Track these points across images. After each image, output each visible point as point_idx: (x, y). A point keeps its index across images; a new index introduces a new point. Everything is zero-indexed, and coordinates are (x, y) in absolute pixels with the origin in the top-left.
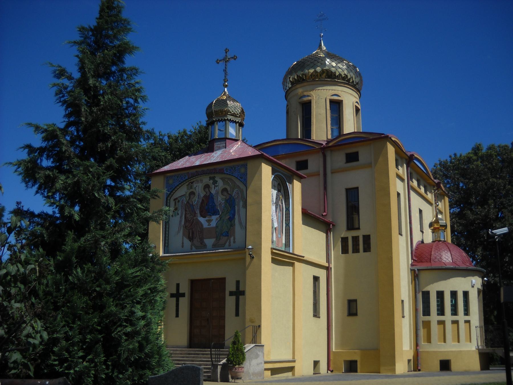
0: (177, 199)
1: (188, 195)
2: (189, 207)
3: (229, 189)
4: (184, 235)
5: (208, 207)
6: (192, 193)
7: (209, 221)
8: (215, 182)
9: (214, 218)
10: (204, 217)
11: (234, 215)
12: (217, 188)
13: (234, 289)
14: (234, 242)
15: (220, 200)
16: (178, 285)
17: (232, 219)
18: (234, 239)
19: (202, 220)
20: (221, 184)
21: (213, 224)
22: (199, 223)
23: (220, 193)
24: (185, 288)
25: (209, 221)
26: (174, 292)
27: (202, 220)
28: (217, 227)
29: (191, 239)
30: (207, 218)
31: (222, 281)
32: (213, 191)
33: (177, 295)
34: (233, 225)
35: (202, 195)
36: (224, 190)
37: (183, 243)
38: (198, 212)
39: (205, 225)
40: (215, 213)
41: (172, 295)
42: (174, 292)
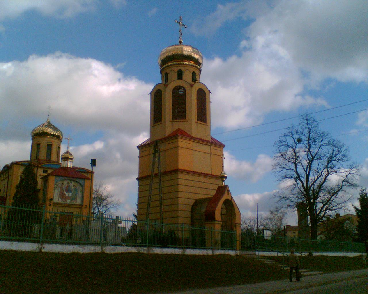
0: (57, 184)
1: (61, 184)
2: (61, 188)
3: (76, 185)
4: (59, 197)
6: (62, 184)
7: (69, 194)
9: (70, 193)
10: (67, 192)
11: (77, 194)
12: (71, 184)
14: (77, 202)
15: (73, 188)
17: (76, 195)
18: (77, 201)
19: (66, 193)
21: (70, 195)
22: (65, 194)
23: (73, 186)
25: (69, 194)
27: (66, 193)
28: (71, 196)
29: (62, 199)
30: (68, 193)
34: (77, 197)
35: (67, 185)
36: (74, 186)
37: (58, 200)
38: (64, 190)
39: (67, 195)
40: (71, 192)
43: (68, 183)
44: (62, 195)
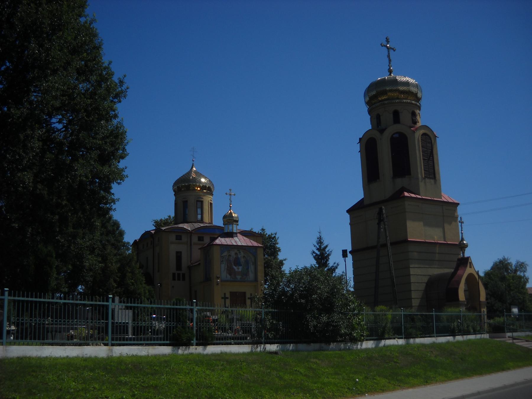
5: (237, 262)
6: (230, 255)
7: (238, 268)
8: (240, 252)
9: (240, 268)
13: (249, 297)
15: (242, 260)
16: (225, 294)
17: (248, 269)
19: (234, 267)
20: (242, 253)
21: (240, 270)
24: (228, 295)
25: (238, 268)
26: (223, 296)
29: (230, 275)
31: (245, 293)
32: (239, 256)
33: (225, 298)
36: (244, 257)
39: (236, 270)
40: (241, 265)
41: (222, 298)
42: (223, 296)
43: (236, 254)
44: (230, 271)
